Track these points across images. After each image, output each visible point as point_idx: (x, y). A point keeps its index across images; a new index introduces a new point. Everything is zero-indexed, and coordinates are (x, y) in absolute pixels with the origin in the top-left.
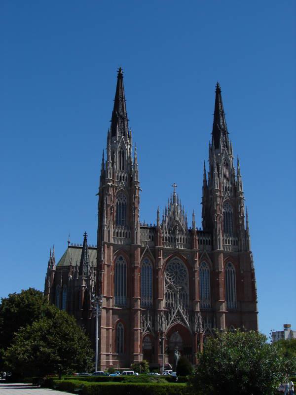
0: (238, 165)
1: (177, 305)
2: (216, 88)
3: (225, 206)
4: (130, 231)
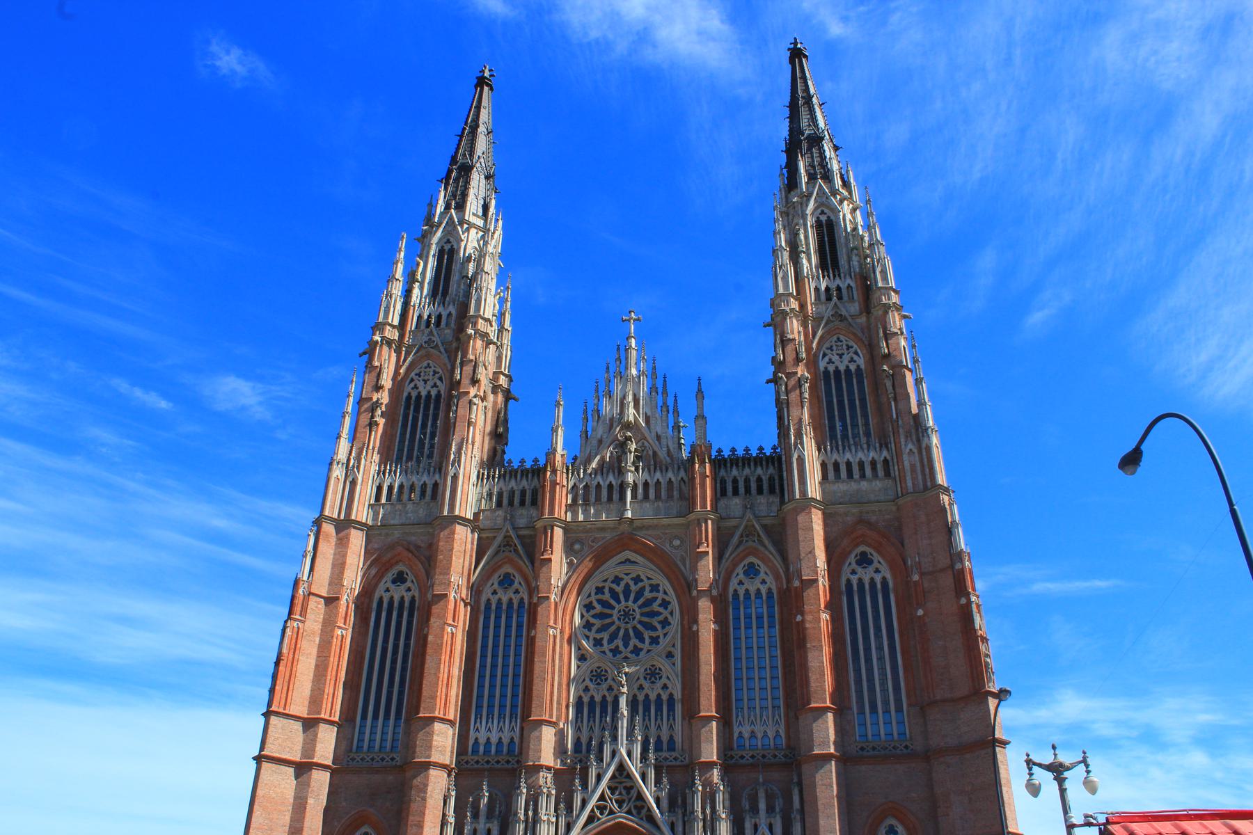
3: (831, 348)
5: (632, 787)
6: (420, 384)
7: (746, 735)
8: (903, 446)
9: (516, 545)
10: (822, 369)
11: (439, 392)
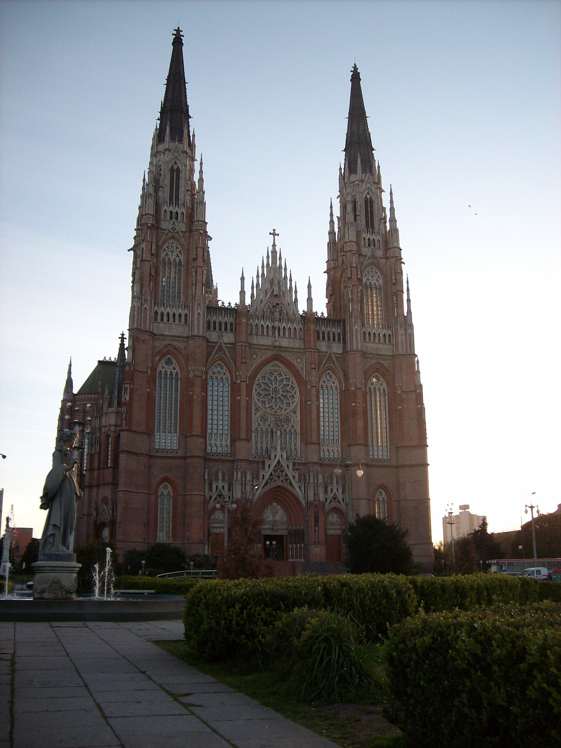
0: (392, 202)
1: (276, 450)
2: (352, 73)
4: (186, 311)
5: (283, 471)
7: (325, 451)
8: (399, 331)
9: (224, 352)
10: (364, 283)
11: (180, 259)
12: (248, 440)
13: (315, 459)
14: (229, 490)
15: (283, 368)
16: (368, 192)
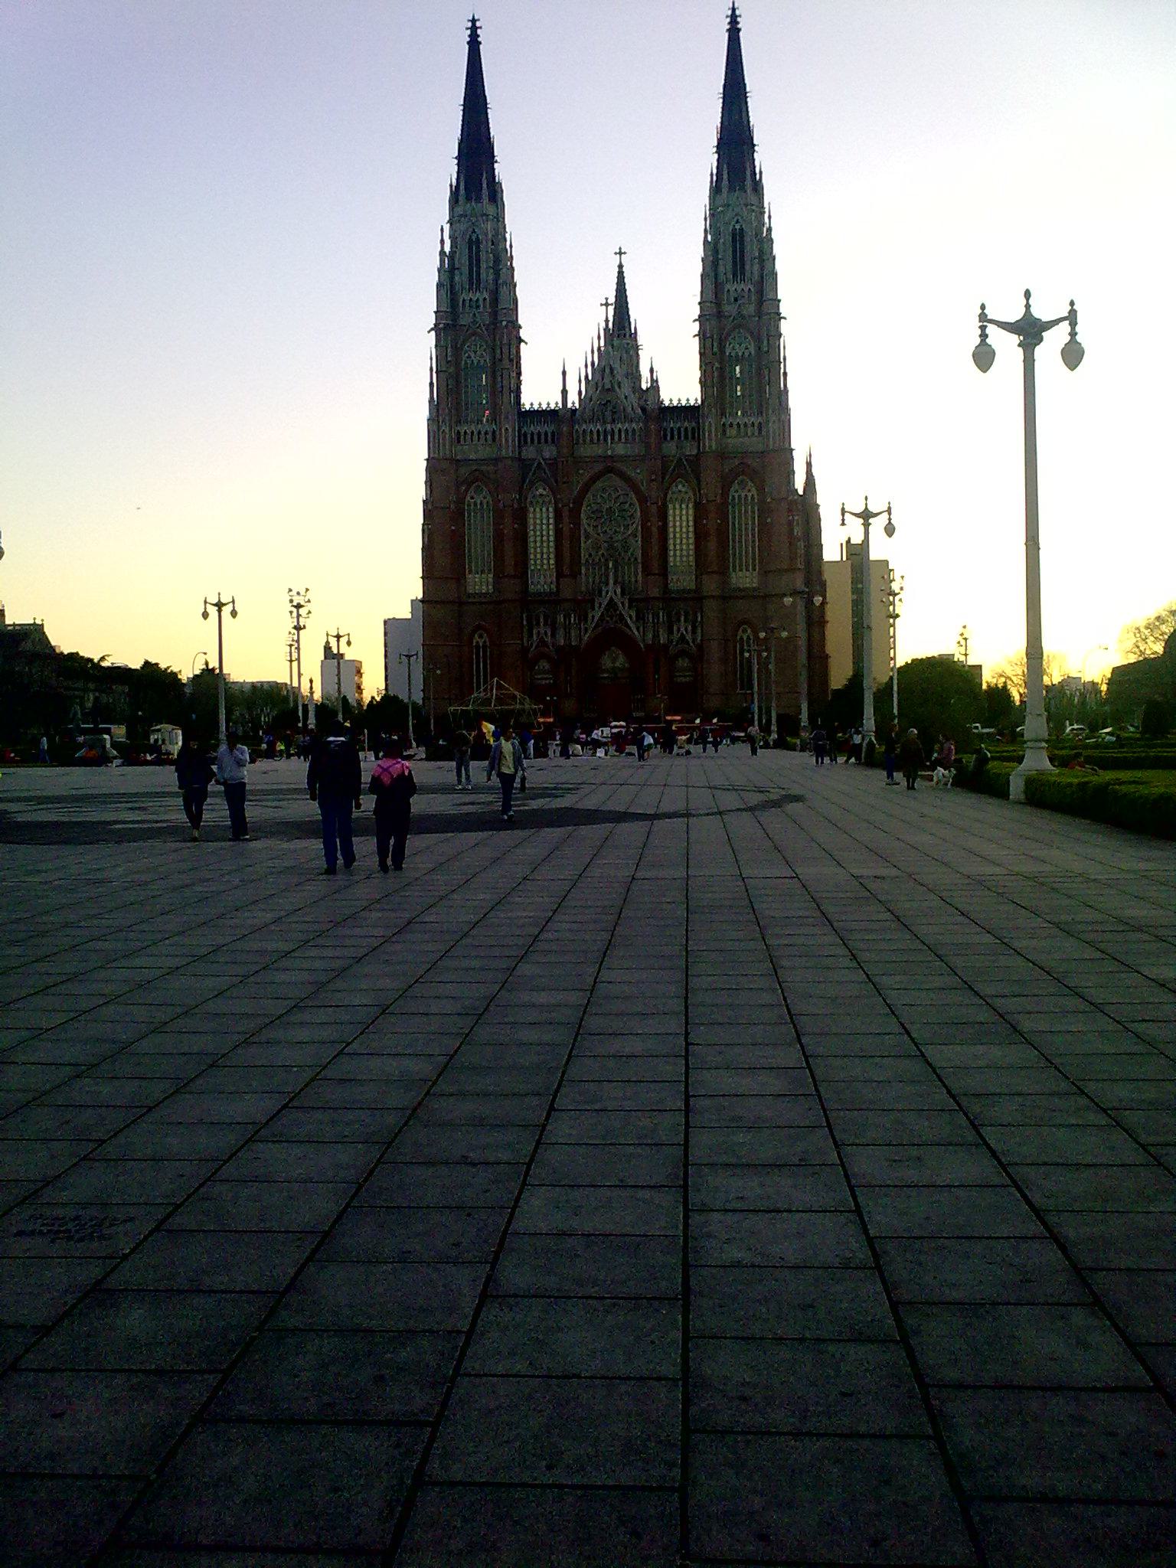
2: (728, 20)
4: (494, 427)
6: (473, 355)
12: (575, 574)
13: (655, 592)
14: (553, 635)
15: (618, 481)
16: (738, 220)
